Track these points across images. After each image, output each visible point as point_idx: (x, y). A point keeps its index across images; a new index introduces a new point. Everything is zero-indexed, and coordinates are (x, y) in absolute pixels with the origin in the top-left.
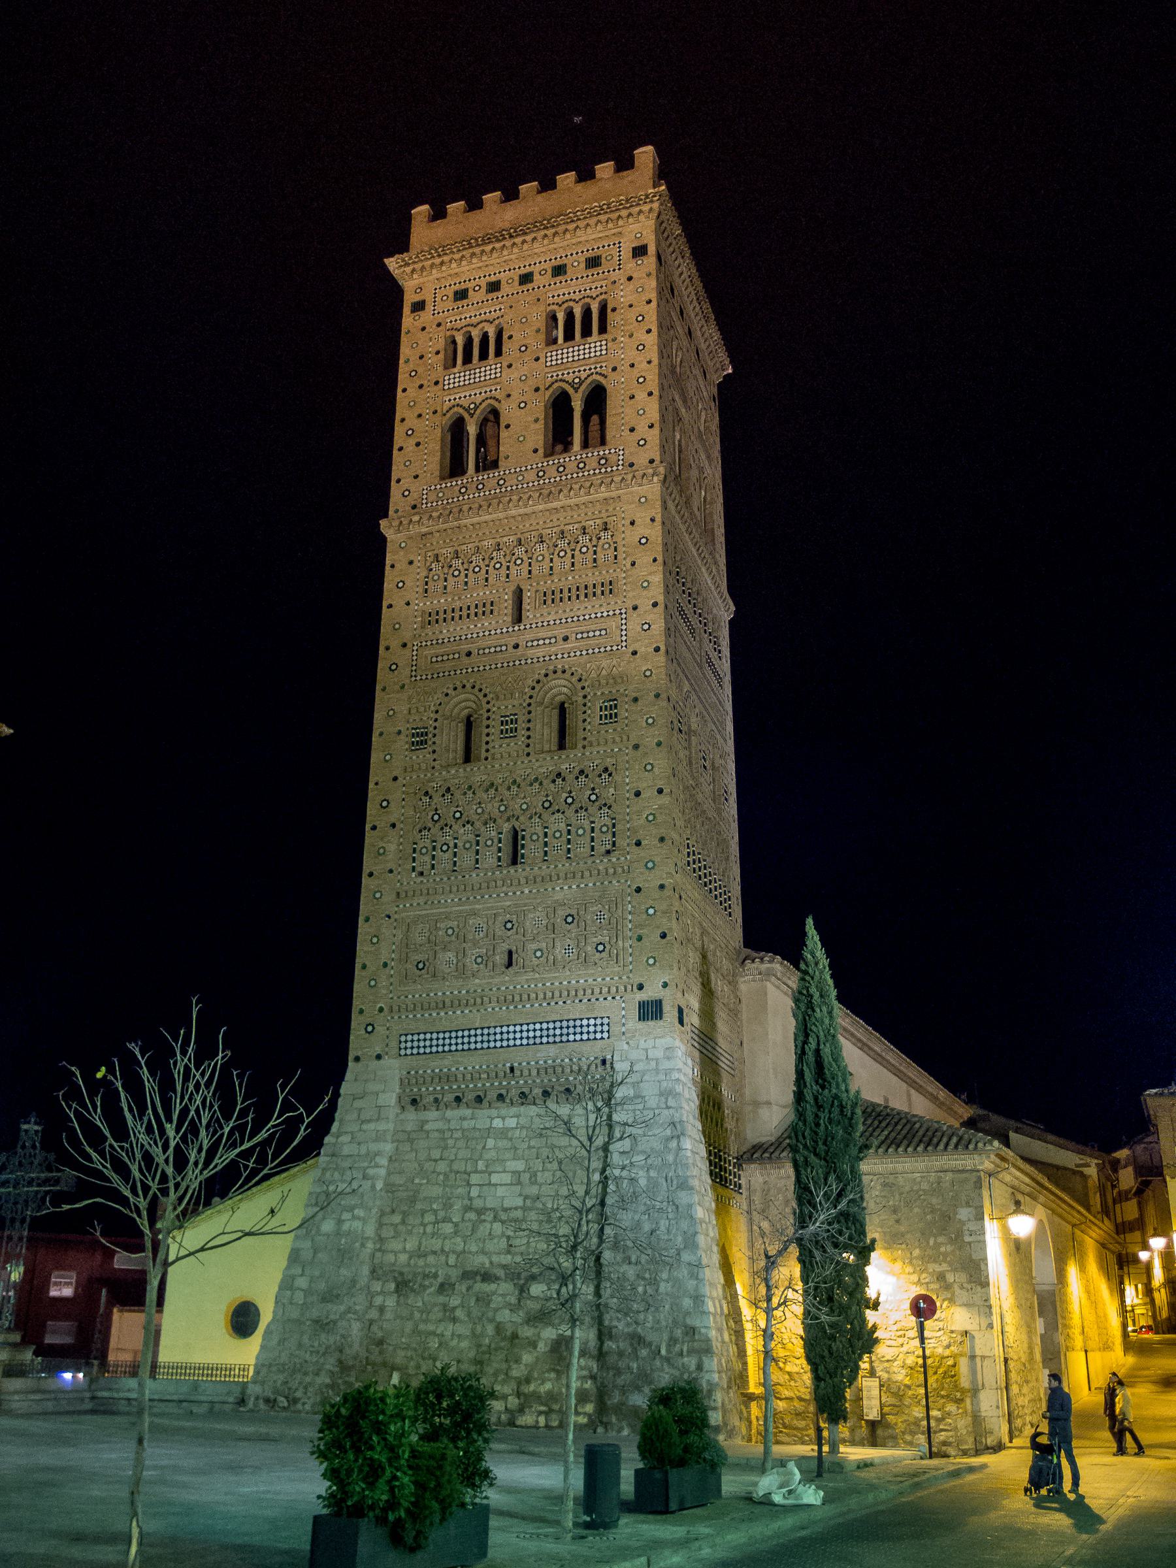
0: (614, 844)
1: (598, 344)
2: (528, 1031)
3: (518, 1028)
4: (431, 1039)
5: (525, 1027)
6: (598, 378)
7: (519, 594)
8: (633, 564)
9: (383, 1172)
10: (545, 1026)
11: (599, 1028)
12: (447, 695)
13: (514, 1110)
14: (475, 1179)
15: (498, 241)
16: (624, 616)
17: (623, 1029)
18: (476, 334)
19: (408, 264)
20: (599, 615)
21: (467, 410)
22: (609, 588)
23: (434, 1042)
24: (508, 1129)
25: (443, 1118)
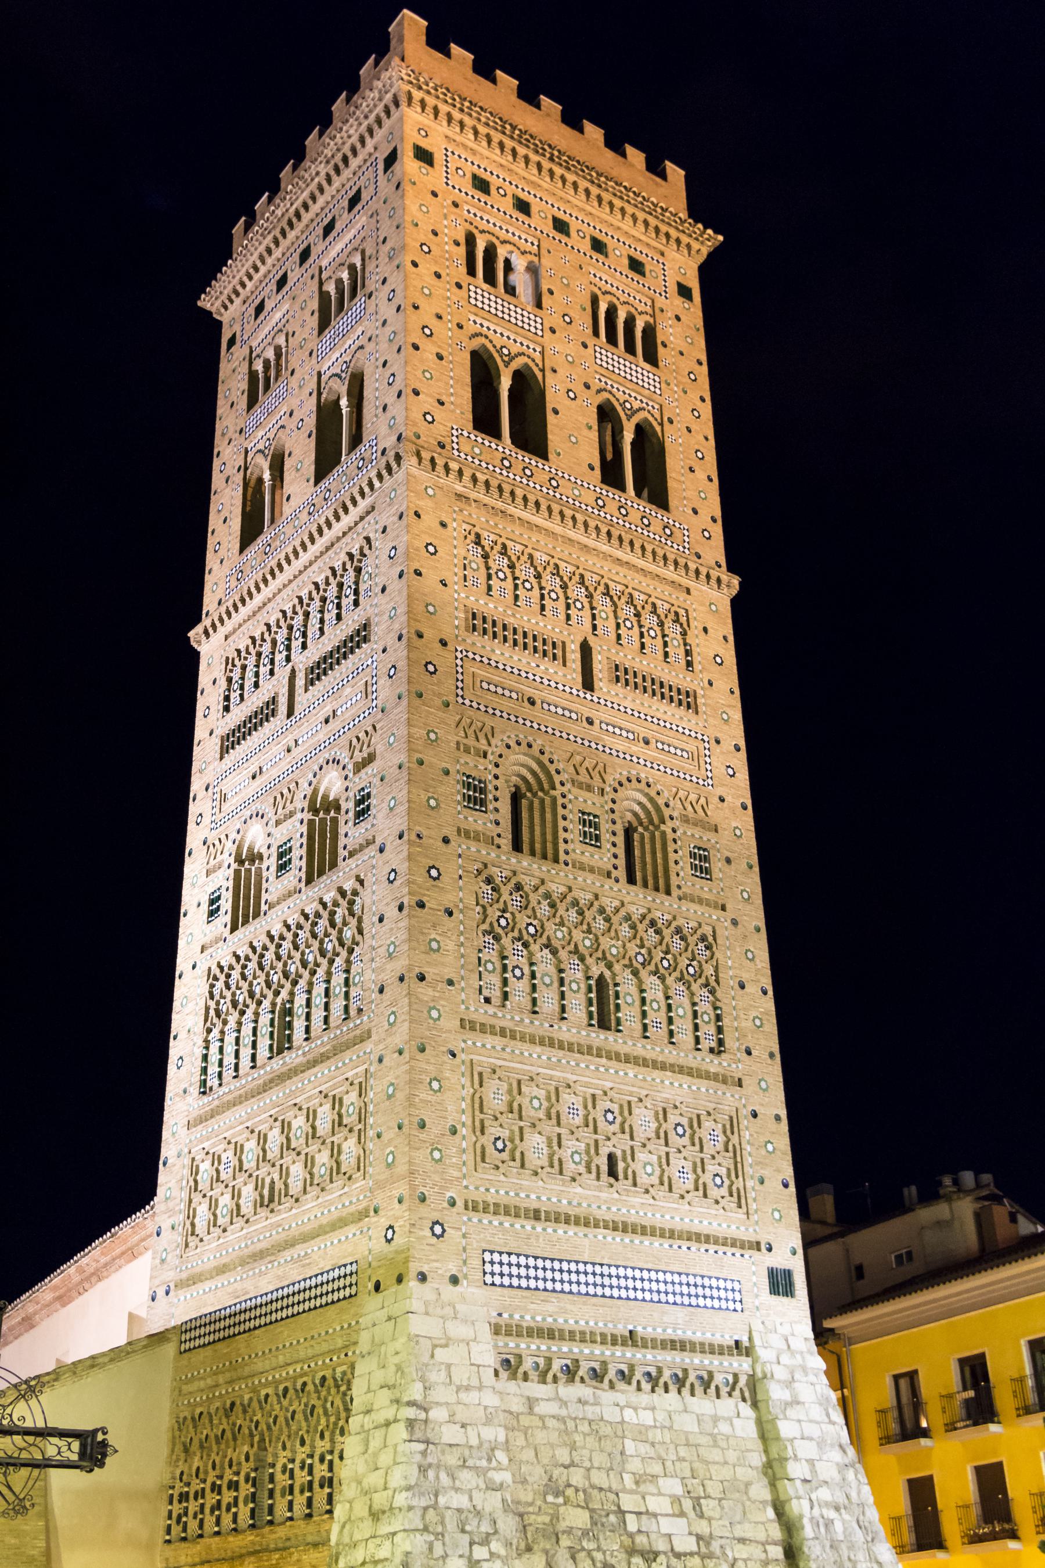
0: (721, 1043)
6: (651, 419)
7: (586, 650)
8: (710, 684)
12: (508, 747)
13: (645, 1398)
14: (628, 1502)
19: (420, 88)
24: (648, 1428)
25: (557, 1398)
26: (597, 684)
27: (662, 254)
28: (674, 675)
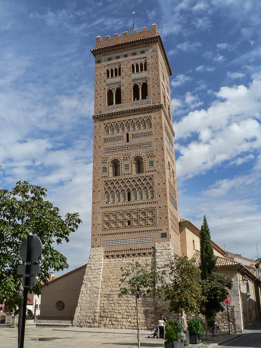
1: (145, 73)
2: (134, 240)
3: (132, 240)
4: (111, 242)
5: (134, 239)
7: (128, 135)
8: (156, 128)
9: (101, 273)
10: (138, 239)
11: (151, 240)
15: (119, 46)
16: (154, 141)
17: (157, 240)
18: (114, 69)
20: (148, 141)
21: (113, 88)
22: (150, 134)
23: (112, 243)
26: (130, 140)
27: (149, 46)
28: (148, 130)
